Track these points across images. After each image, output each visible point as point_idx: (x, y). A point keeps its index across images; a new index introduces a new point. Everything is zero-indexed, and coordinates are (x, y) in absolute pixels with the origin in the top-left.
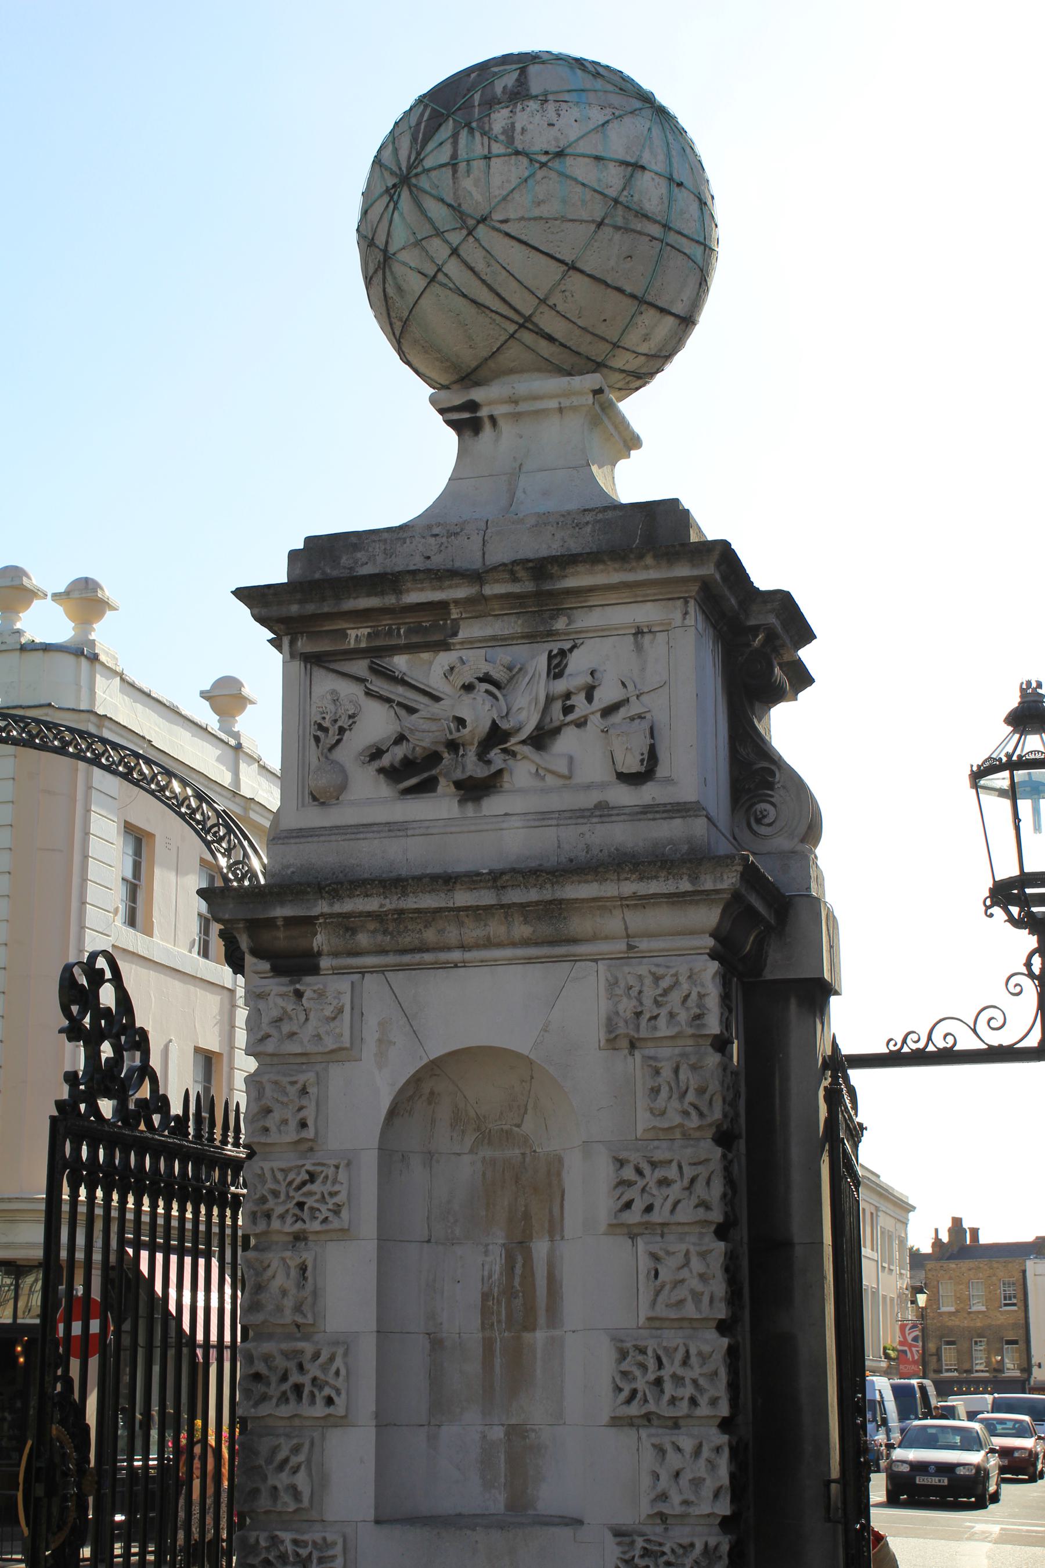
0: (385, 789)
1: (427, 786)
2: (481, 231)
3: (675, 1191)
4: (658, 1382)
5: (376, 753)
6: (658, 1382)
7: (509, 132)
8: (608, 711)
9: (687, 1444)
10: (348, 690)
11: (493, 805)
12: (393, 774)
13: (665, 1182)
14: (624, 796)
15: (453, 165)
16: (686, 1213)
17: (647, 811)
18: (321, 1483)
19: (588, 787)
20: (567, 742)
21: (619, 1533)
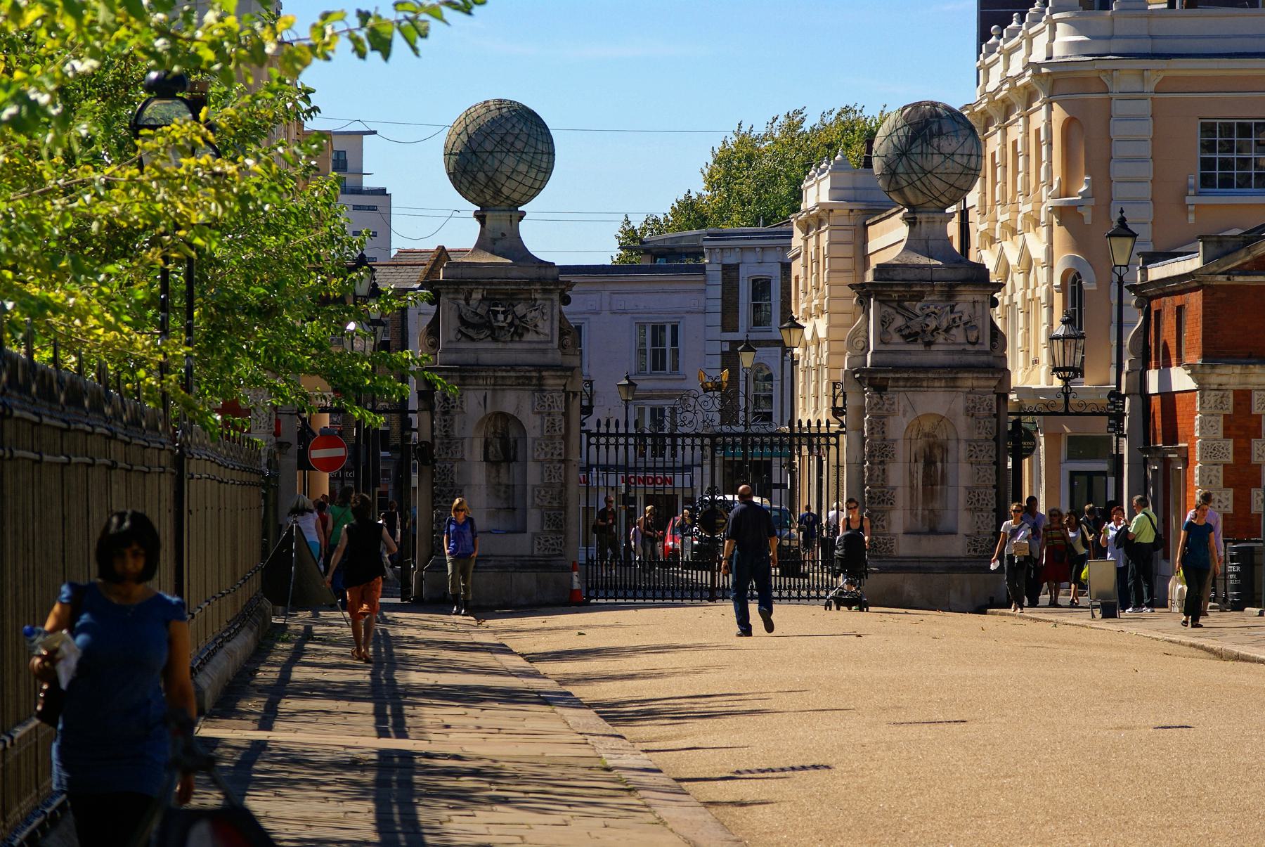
0: (902, 341)
1: (915, 341)
2: (929, 175)
3: (984, 453)
4: (978, 500)
5: (899, 330)
6: (978, 500)
7: (939, 146)
8: (965, 324)
9: (985, 515)
10: (890, 310)
11: (934, 348)
12: (905, 337)
13: (981, 451)
14: (969, 347)
15: (922, 153)
16: (987, 459)
17: (977, 353)
18: (889, 524)
19: (960, 344)
20: (954, 331)
21: (967, 536)
